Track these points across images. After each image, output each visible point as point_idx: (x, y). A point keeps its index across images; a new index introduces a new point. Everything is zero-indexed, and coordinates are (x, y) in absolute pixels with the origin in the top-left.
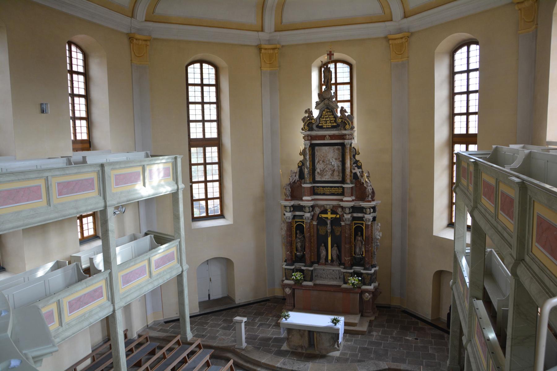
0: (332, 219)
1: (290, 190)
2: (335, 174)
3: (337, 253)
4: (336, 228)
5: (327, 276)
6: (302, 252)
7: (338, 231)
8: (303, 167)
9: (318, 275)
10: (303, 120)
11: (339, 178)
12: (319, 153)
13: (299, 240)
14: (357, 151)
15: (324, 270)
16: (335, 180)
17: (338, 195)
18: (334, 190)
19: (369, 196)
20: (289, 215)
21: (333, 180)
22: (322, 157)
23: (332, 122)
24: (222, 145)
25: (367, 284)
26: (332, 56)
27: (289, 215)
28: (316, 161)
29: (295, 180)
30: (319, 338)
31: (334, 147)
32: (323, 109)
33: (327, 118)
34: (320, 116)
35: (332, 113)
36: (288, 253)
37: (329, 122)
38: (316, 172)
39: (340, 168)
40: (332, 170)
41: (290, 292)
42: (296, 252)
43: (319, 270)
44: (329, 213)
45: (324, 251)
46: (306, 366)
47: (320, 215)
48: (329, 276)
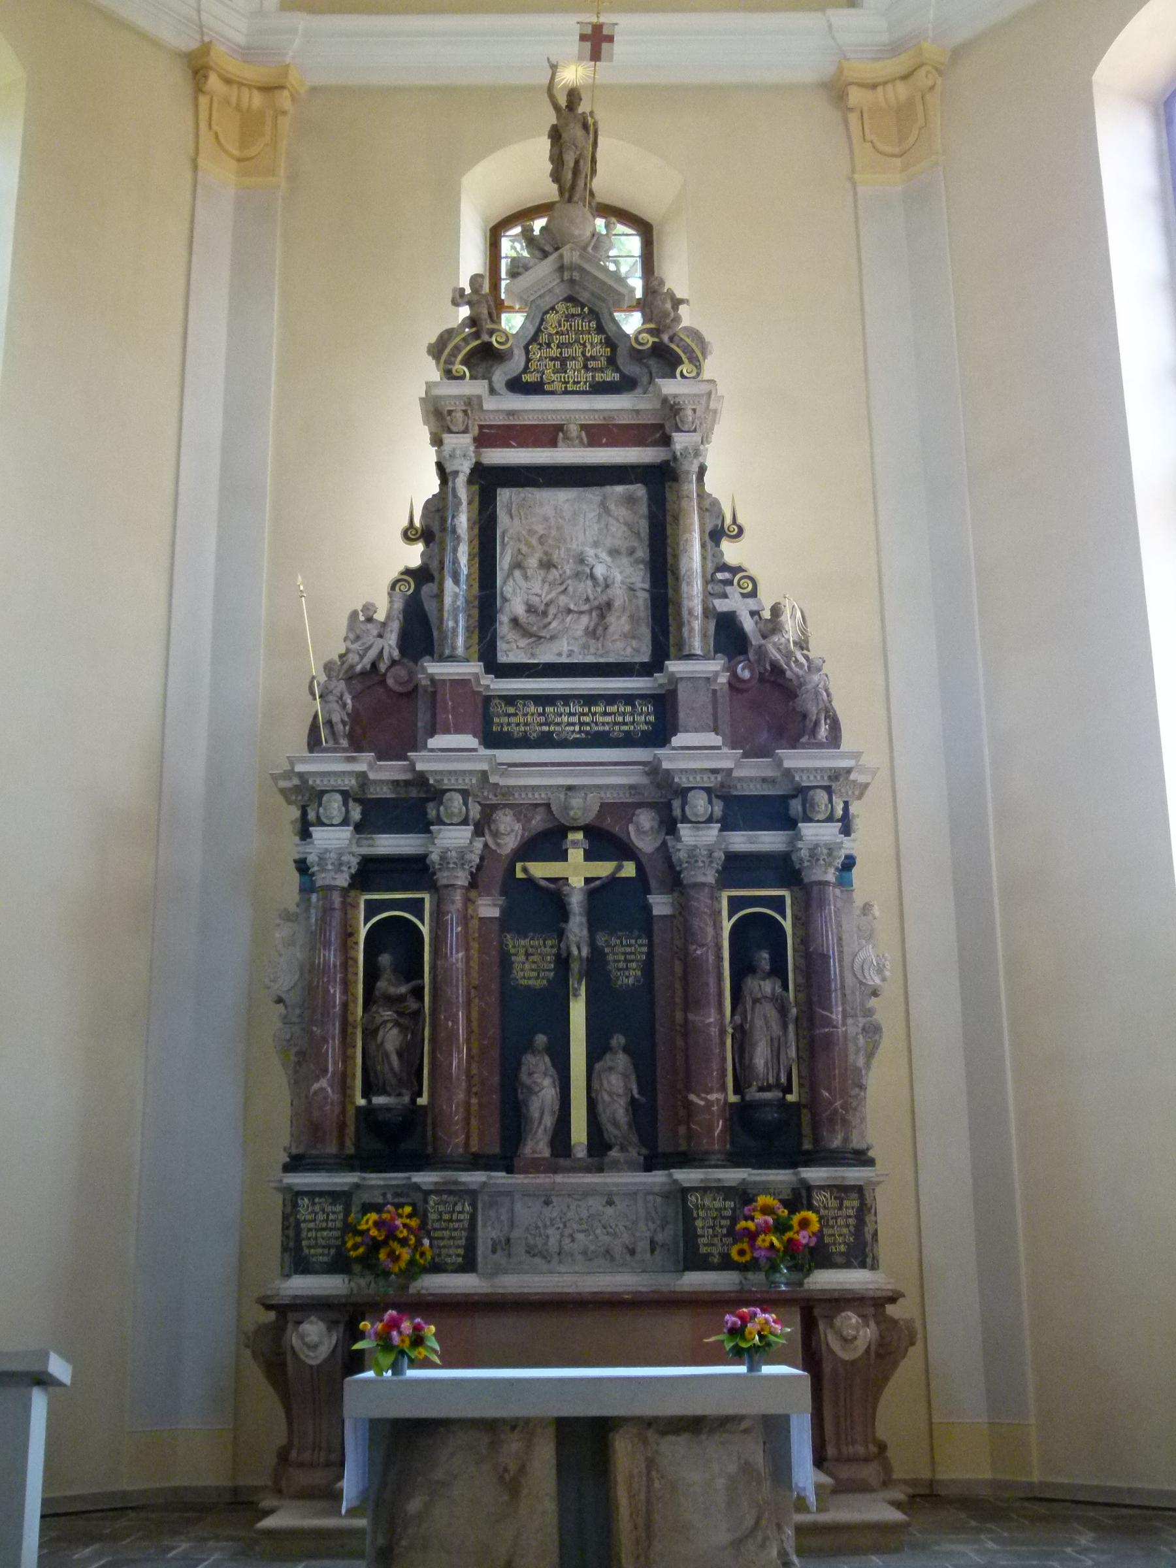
0: (598, 883)
1: (349, 701)
2: (612, 629)
4: (614, 941)
7: (626, 961)
9: (508, 1240)
10: (437, 350)
11: (637, 650)
12: (516, 521)
13: (388, 1014)
14: (728, 520)
15: (547, 1203)
16: (611, 660)
17: (628, 741)
18: (605, 714)
19: (816, 724)
21: (602, 660)
22: (534, 541)
23: (591, 364)
25: (839, 1260)
26: (605, 46)
28: (504, 562)
29: (381, 652)
31: (608, 489)
32: (548, 302)
33: (568, 345)
34: (532, 332)
35: (593, 324)
36: (316, 1086)
37: (578, 364)
38: (503, 619)
39: (643, 598)
40: (599, 608)
41: (324, 1351)
42: (362, 1102)
43: (518, 1206)
44: (576, 855)
45: (547, 1082)
47: (519, 866)
48: (580, 1236)
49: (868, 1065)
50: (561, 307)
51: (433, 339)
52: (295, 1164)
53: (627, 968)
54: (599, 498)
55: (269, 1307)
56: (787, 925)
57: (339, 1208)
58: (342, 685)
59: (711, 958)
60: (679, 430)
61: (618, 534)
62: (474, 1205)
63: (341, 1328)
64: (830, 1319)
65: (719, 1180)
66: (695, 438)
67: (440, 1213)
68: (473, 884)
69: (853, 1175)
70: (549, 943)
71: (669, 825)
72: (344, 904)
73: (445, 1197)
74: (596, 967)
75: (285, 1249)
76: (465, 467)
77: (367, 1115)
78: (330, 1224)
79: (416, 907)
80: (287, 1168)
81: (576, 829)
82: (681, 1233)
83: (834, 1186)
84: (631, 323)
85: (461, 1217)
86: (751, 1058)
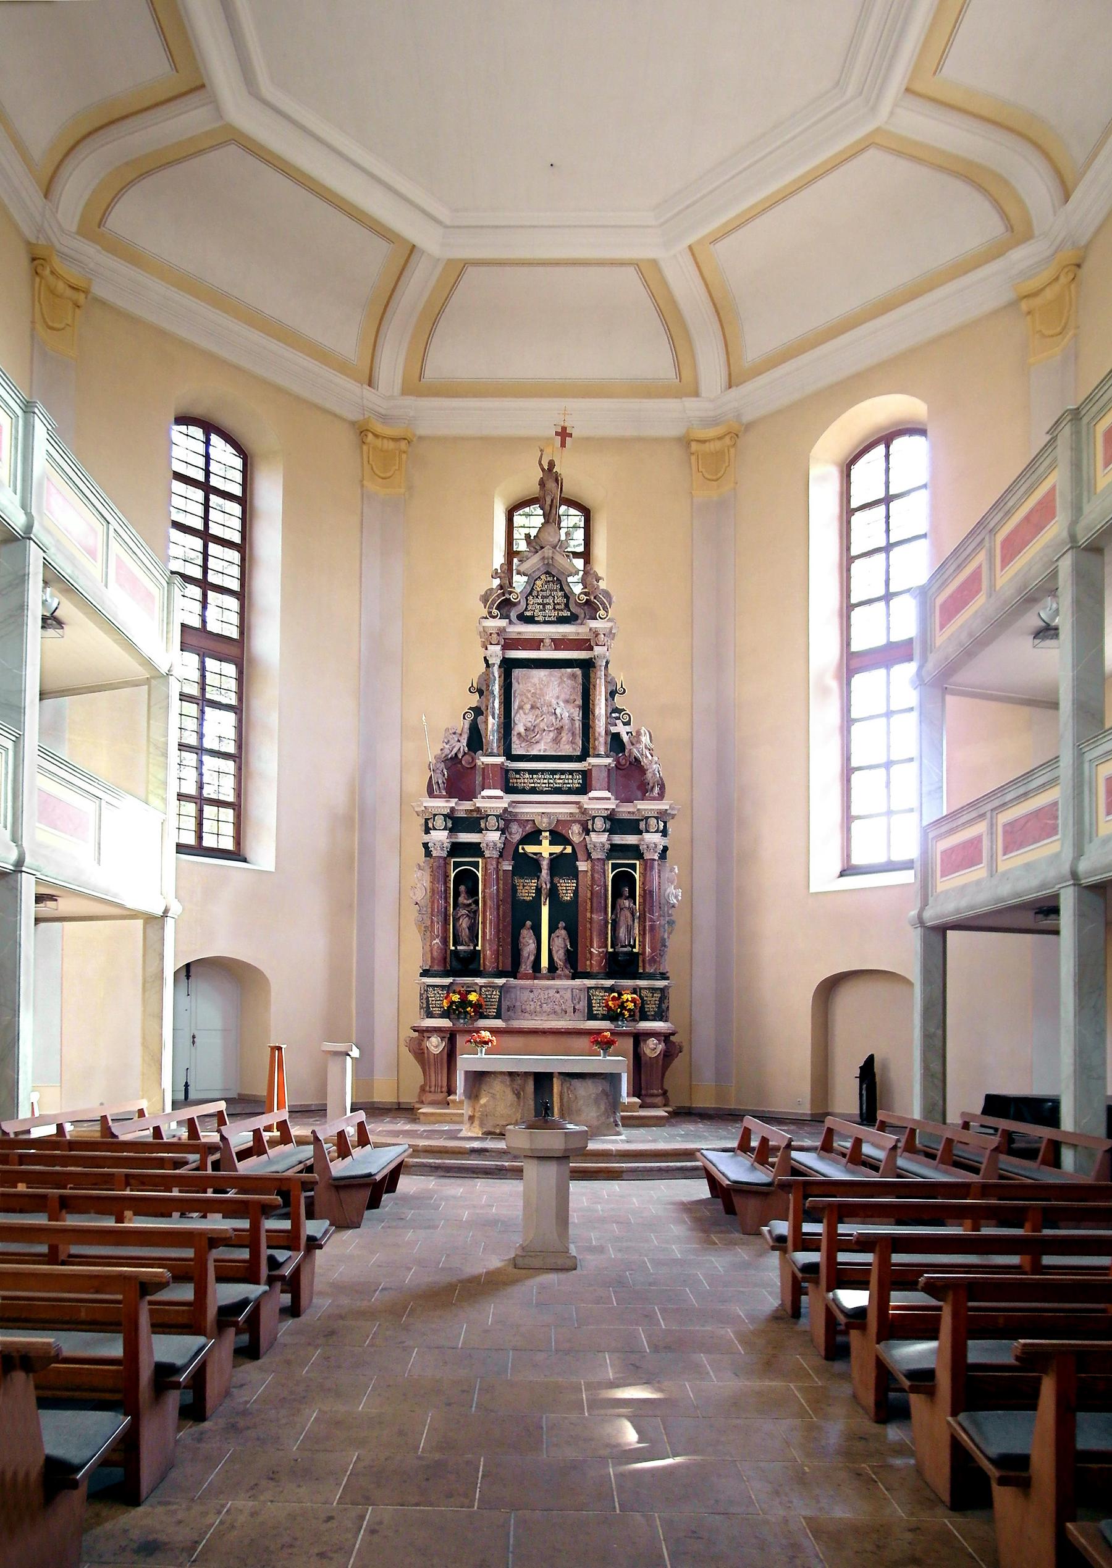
2: (564, 739)
5: (541, 1006)
7: (566, 890)
8: (480, 719)
11: (574, 749)
12: (521, 686)
15: (531, 992)
17: (570, 792)
18: (560, 779)
19: (653, 788)
20: (440, 837)
22: (529, 695)
23: (557, 607)
24: (250, 661)
25: (651, 1018)
27: (440, 837)
28: (515, 705)
32: (537, 574)
33: (547, 597)
34: (529, 589)
35: (558, 586)
36: (435, 942)
38: (514, 733)
39: (578, 724)
42: (453, 948)
43: (518, 993)
44: (546, 843)
45: (531, 941)
47: (520, 847)
52: (425, 973)
55: (415, 1031)
56: (637, 876)
58: (443, 765)
59: (603, 891)
60: (597, 645)
62: (500, 992)
63: (446, 1040)
64: (645, 1041)
66: (605, 648)
68: (501, 856)
71: (587, 832)
74: (553, 893)
75: (421, 1008)
76: (496, 661)
77: (455, 953)
79: (476, 865)
80: (422, 975)
84: (577, 589)
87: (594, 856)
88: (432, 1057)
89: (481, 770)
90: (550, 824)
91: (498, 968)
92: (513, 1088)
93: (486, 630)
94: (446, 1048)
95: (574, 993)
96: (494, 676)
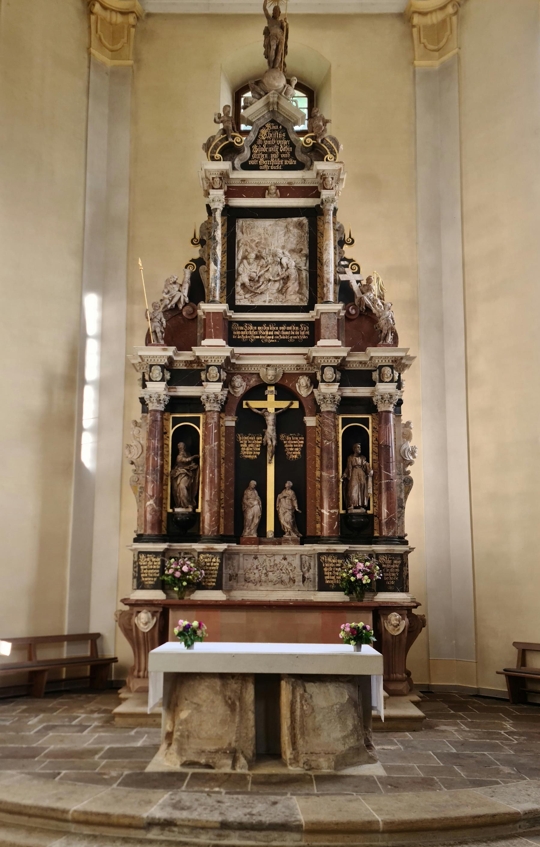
0: (281, 410)
1: (164, 322)
2: (290, 289)
3: (294, 507)
5: (266, 575)
6: (190, 506)
7: (293, 447)
9: (237, 575)
11: (301, 300)
12: (245, 234)
14: (347, 236)
15: (256, 558)
16: (289, 304)
18: (286, 330)
19: (387, 335)
21: (285, 304)
22: (253, 245)
23: (283, 156)
25: (391, 588)
28: (239, 255)
29: (180, 299)
30: (302, 705)
31: (289, 220)
32: (262, 122)
35: (284, 135)
38: (239, 283)
39: (305, 274)
40: (283, 279)
42: (170, 511)
43: (241, 559)
44: (271, 397)
45: (256, 503)
46: (279, 806)
47: (244, 402)
48: (270, 574)
49: (406, 498)
50: (268, 126)
51: (205, 142)
52: (139, 539)
53: (294, 451)
54: (285, 224)
56: (370, 432)
57: (159, 559)
59: (333, 446)
61: (293, 243)
62: (221, 559)
65: (335, 550)
66: (332, 192)
67: (205, 562)
69: (399, 549)
70: (258, 438)
71: (314, 383)
72: (162, 418)
73: (208, 555)
74: (279, 450)
75: (134, 577)
77: (171, 516)
78: (154, 567)
79: (196, 421)
80: (136, 540)
81: (271, 385)
82: (317, 573)
83: (390, 554)
85: (215, 564)
86: (351, 493)
87: (324, 408)
88: (141, 635)
89: (202, 322)
90: (276, 376)
91: (218, 531)
92: (225, 696)
93: (208, 175)
94: (157, 626)
95: (303, 559)
96: (215, 221)
